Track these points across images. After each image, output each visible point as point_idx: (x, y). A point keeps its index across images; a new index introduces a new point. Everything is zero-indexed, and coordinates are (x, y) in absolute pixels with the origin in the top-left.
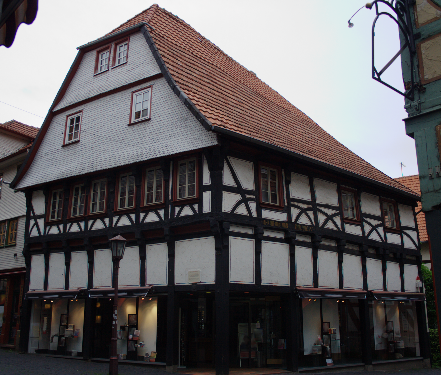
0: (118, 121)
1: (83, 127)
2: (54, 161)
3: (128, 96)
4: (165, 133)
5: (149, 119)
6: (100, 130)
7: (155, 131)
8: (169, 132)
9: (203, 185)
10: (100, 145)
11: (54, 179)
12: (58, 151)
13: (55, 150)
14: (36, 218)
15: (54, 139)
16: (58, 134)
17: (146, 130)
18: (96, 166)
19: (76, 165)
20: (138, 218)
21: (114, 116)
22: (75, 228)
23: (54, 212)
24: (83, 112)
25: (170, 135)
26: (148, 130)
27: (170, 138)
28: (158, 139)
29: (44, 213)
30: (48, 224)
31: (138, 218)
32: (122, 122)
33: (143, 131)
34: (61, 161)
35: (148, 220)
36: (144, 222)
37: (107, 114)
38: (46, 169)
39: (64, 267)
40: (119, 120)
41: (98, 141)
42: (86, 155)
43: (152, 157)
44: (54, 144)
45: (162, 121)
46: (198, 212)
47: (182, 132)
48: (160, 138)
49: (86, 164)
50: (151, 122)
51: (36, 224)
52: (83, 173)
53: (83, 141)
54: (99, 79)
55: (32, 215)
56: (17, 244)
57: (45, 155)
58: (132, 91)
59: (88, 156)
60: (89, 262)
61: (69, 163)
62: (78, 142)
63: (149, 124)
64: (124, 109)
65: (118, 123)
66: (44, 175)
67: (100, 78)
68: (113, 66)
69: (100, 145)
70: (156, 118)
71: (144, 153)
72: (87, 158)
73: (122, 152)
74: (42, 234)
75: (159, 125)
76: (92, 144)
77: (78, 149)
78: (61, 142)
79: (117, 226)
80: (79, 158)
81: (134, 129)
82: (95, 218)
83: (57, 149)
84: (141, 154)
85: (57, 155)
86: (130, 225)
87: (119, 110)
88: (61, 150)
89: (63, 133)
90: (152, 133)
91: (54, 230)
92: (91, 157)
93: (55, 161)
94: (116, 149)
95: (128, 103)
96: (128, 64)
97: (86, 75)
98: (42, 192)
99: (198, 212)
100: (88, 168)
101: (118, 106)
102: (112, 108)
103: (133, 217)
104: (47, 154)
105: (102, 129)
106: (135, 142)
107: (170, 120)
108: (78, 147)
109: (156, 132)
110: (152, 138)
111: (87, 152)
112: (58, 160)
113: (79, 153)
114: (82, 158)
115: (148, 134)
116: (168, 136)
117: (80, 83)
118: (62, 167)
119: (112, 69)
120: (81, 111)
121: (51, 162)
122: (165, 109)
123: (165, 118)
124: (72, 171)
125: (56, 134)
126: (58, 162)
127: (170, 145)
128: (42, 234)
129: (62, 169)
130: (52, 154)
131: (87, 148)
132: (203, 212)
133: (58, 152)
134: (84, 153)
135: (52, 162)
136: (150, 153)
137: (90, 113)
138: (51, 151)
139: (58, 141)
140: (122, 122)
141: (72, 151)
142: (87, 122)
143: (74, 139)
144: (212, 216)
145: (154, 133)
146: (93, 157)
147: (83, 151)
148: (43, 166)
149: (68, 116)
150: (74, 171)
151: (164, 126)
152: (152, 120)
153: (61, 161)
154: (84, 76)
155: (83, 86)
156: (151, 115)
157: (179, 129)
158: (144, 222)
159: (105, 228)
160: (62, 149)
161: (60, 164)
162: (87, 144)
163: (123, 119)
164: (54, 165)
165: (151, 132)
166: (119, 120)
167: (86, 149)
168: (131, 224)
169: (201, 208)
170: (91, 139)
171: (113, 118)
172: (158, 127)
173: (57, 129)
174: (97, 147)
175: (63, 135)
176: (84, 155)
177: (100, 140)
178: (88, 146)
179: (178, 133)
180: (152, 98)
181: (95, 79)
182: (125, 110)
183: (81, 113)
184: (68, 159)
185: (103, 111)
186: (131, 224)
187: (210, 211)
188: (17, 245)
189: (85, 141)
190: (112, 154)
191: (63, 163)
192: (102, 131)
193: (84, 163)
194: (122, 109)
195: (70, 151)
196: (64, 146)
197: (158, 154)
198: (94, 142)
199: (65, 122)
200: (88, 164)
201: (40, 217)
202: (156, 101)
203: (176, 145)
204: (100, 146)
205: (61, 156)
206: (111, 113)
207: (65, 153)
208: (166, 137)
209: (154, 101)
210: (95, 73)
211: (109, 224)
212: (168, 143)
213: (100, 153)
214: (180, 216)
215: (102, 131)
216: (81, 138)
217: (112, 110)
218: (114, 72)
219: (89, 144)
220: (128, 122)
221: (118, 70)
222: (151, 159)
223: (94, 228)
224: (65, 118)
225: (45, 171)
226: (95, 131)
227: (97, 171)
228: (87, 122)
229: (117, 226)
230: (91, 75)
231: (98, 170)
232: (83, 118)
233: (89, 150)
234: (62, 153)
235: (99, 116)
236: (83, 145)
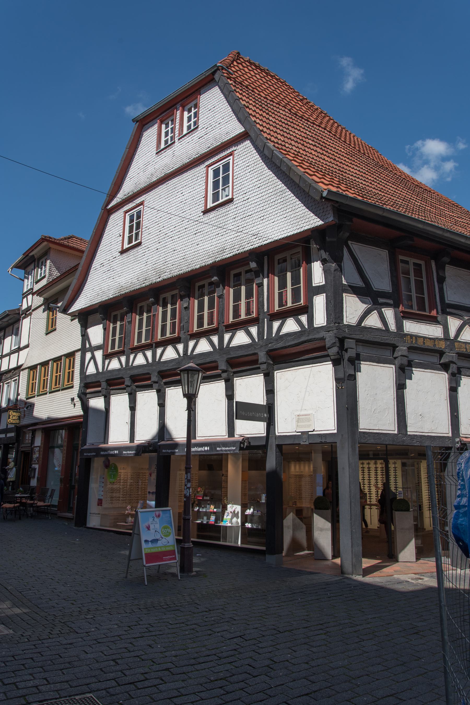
0: (189, 208)
1: (145, 224)
2: (111, 273)
3: (202, 173)
4: (254, 215)
5: (231, 201)
6: (167, 224)
7: (239, 215)
8: (260, 213)
9: (314, 285)
10: (167, 244)
11: (111, 297)
12: (115, 259)
13: (112, 258)
14: (93, 349)
15: (110, 244)
16: (114, 237)
17: (228, 216)
18: (162, 273)
19: (138, 275)
20: (221, 340)
21: (184, 202)
22: (140, 360)
23: (114, 341)
24: (145, 203)
25: (262, 218)
26: (231, 215)
27: (261, 222)
28: (245, 225)
29: (102, 343)
30: (107, 356)
31: (221, 340)
32: (194, 209)
33: (223, 218)
34: (119, 272)
35: (235, 343)
36: (231, 346)
37: (175, 201)
38: (102, 284)
39: (128, 412)
40: (191, 207)
41: (165, 239)
42: (150, 260)
43: (237, 252)
44: (110, 252)
45: (249, 200)
46: (307, 327)
47: (279, 211)
48: (248, 224)
49: (150, 273)
50: (234, 204)
51: (93, 357)
52: (147, 284)
53: (146, 242)
54: (162, 157)
55: (88, 346)
56: (74, 385)
57: (100, 266)
58: (206, 164)
59: (152, 261)
60: (159, 405)
61: (129, 274)
62: (139, 244)
63: (231, 207)
64: (197, 191)
65: (190, 211)
66: (99, 292)
67: (164, 154)
68: (179, 135)
69: (167, 244)
70: (242, 197)
71: (225, 248)
72: (151, 265)
73: (196, 250)
74: (101, 370)
75: (246, 205)
76: (158, 245)
77: (139, 253)
78: (119, 248)
79: (194, 354)
80: (141, 266)
81: (211, 216)
82: (164, 343)
83: (115, 256)
84: (222, 249)
85: (114, 264)
86: (211, 352)
87: (190, 194)
88: (118, 257)
89: (120, 236)
90: (237, 219)
91: (114, 364)
92: (157, 262)
93: (112, 273)
94: (188, 247)
95: (201, 182)
96: (199, 129)
97: (147, 155)
98: (99, 316)
99: (307, 327)
100: (152, 276)
101: (188, 189)
102: (182, 192)
103: (215, 339)
104: (102, 265)
105: (169, 223)
106: (213, 235)
107: (260, 196)
108: (140, 250)
109: (242, 217)
110: (236, 226)
111: (151, 257)
112: (115, 272)
113: (141, 258)
114: (145, 265)
115: (231, 221)
116: (259, 219)
117: (140, 167)
118: (121, 279)
119: (179, 139)
120: (142, 203)
121: (107, 275)
122: (254, 181)
123: (253, 195)
124: (134, 283)
125: (113, 238)
126: (116, 274)
127: (263, 231)
128: (101, 370)
129: (120, 282)
130: (108, 265)
131: (151, 251)
132: (315, 326)
133: (116, 261)
134: (147, 258)
135: (108, 274)
136: (235, 247)
137: (153, 204)
138: (107, 260)
139: (115, 247)
140: (194, 209)
141: (132, 257)
142: (149, 217)
143: (135, 241)
144: (329, 331)
145: (239, 218)
146: (159, 261)
147: (146, 256)
148: (98, 281)
149: (126, 212)
150: (136, 283)
151: (253, 206)
152: (235, 200)
153: (119, 272)
154: (144, 157)
155: (142, 170)
156: (234, 194)
158: (231, 346)
159: (178, 357)
160: (120, 257)
161: (118, 275)
162: (151, 245)
163: (196, 205)
164: (111, 278)
165: (234, 216)
166: (191, 207)
167: (149, 252)
168: (212, 350)
169: (311, 320)
170: (155, 238)
171: (184, 205)
172: (244, 209)
173: (113, 231)
174: (164, 248)
175: (121, 238)
176: (148, 260)
177: (167, 238)
178: (152, 248)
179: (274, 214)
180: (235, 169)
181: (158, 157)
182: (199, 193)
183: (142, 206)
184: (128, 269)
185: (169, 198)
186: (212, 350)
187: (325, 324)
188: (74, 387)
189: (148, 241)
190: (183, 254)
191: (122, 274)
192: (169, 226)
193: (148, 271)
194: (195, 192)
195: (130, 258)
196: (123, 252)
197: (246, 246)
198: (159, 242)
199: (123, 220)
200: (153, 271)
201: (98, 348)
202: (240, 172)
203: (270, 231)
204: (168, 246)
205: (119, 265)
206: (179, 199)
207: (123, 261)
208: (256, 220)
209: (237, 173)
210: (157, 150)
211: (184, 351)
212: (259, 230)
213: (168, 255)
214: (281, 334)
215: (169, 226)
216: (143, 239)
217: (181, 195)
218: (181, 143)
219: (153, 244)
220: (203, 208)
221: (187, 139)
222: (236, 254)
223: (164, 358)
224: (123, 215)
225: (101, 287)
226: (161, 227)
227: (164, 280)
228: (149, 217)
229: (194, 354)
230: (152, 153)
231: (165, 277)
232: (145, 211)
233: (154, 253)
234: (120, 262)
235: (165, 206)
236: (145, 248)
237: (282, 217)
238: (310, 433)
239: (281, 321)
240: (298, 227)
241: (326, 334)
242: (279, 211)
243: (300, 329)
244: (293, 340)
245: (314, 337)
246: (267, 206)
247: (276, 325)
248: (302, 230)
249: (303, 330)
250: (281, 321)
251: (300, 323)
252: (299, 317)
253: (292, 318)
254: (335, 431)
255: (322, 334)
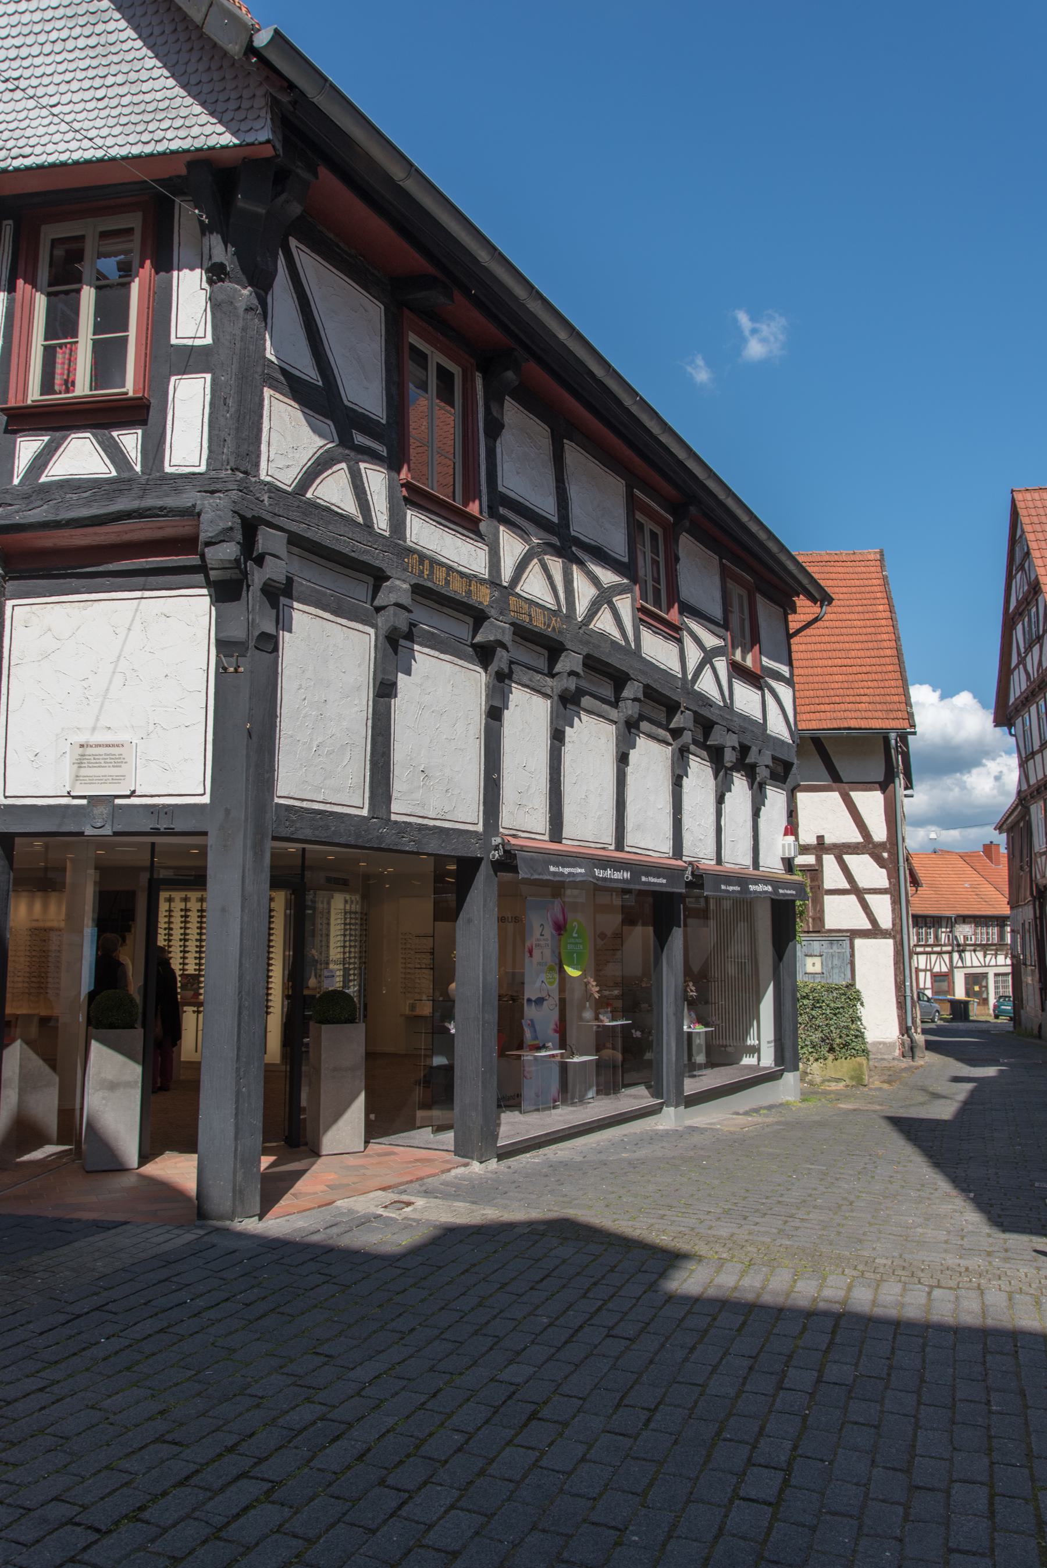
46: (138, 468)
47: (80, 75)
132: (168, 469)
144: (213, 492)
157: (59, 58)
187: (203, 469)
203: (41, 131)
214: (43, 479)
237: (88, 95)
238: (118, 801)
239: (46, 439)
240: (146, 137)
241: (204, 498)
242: (80, 75)
243: (114, 473)
244: (88, 502)
245: (160, 503)
246: (36, 50)
247: (27, 448)
248: (161, 148)
249: (126, 475)
250: (46, 439)
251: (115, 453)
252: (115, 434)
253: (88, 435)
254: (206, 799)
255: (189, 498)
